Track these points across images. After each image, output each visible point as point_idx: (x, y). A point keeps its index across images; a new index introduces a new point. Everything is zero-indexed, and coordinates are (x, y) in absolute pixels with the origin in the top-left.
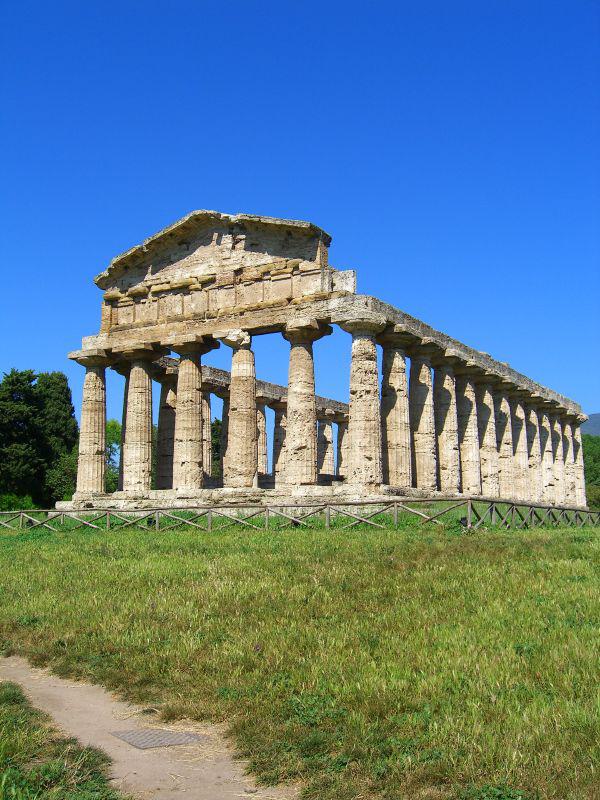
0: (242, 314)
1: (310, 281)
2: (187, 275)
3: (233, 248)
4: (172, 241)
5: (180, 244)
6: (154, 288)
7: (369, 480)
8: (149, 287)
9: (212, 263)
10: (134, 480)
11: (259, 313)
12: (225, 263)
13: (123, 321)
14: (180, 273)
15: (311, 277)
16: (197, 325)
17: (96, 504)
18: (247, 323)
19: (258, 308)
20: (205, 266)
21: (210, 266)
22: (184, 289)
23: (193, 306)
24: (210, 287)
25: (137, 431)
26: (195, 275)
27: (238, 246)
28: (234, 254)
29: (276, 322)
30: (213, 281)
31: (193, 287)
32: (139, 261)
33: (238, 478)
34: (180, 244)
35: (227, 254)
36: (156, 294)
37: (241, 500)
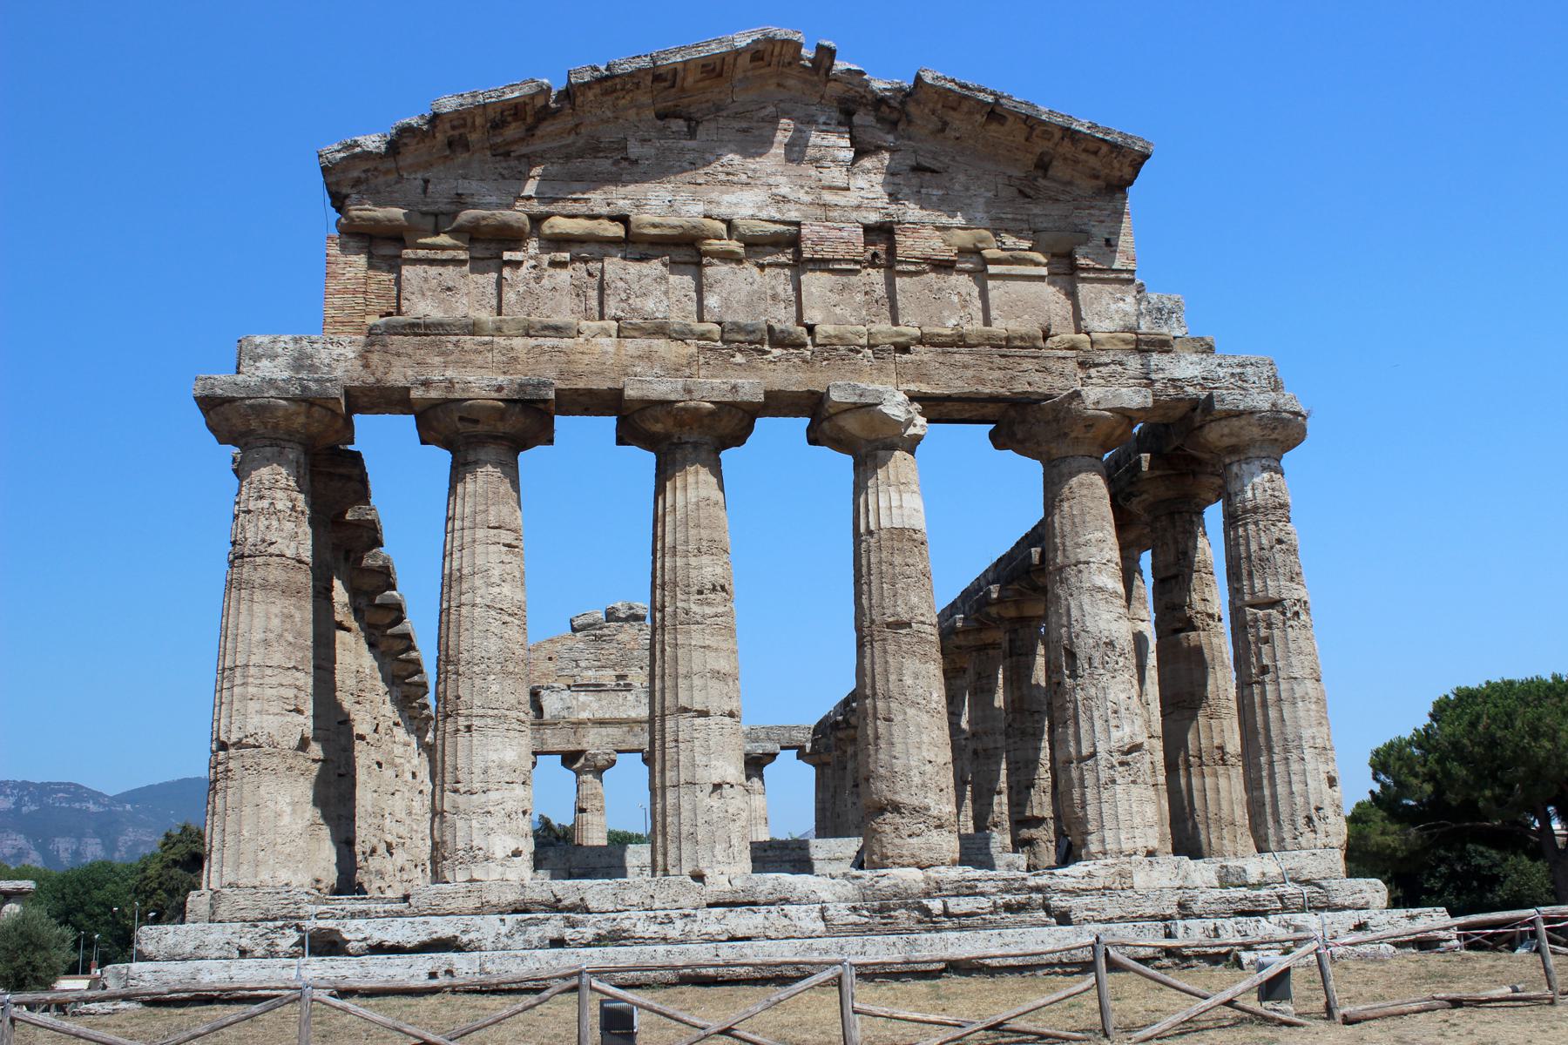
0: (904, 349)
1: (1106, 299)
4: (645, 99)
5: (662, 116)
9: (784, 190)
10: (501, 845)
11: (962, 356)
12: (828, 197)
13: (422, 307)
15: (1108, 288)
16: (739, 358)
17: (355, 931)
18: (922, 377)
19: (960, 341)
22: (685, 249)
24: (768, 259)
26: (724, 211)
27: (867, 163)
28: (860, 181)
29: (1020, 387)
31: (715, 245)
32: (513, 131)
33: (935, 837)
34: (662, 116)
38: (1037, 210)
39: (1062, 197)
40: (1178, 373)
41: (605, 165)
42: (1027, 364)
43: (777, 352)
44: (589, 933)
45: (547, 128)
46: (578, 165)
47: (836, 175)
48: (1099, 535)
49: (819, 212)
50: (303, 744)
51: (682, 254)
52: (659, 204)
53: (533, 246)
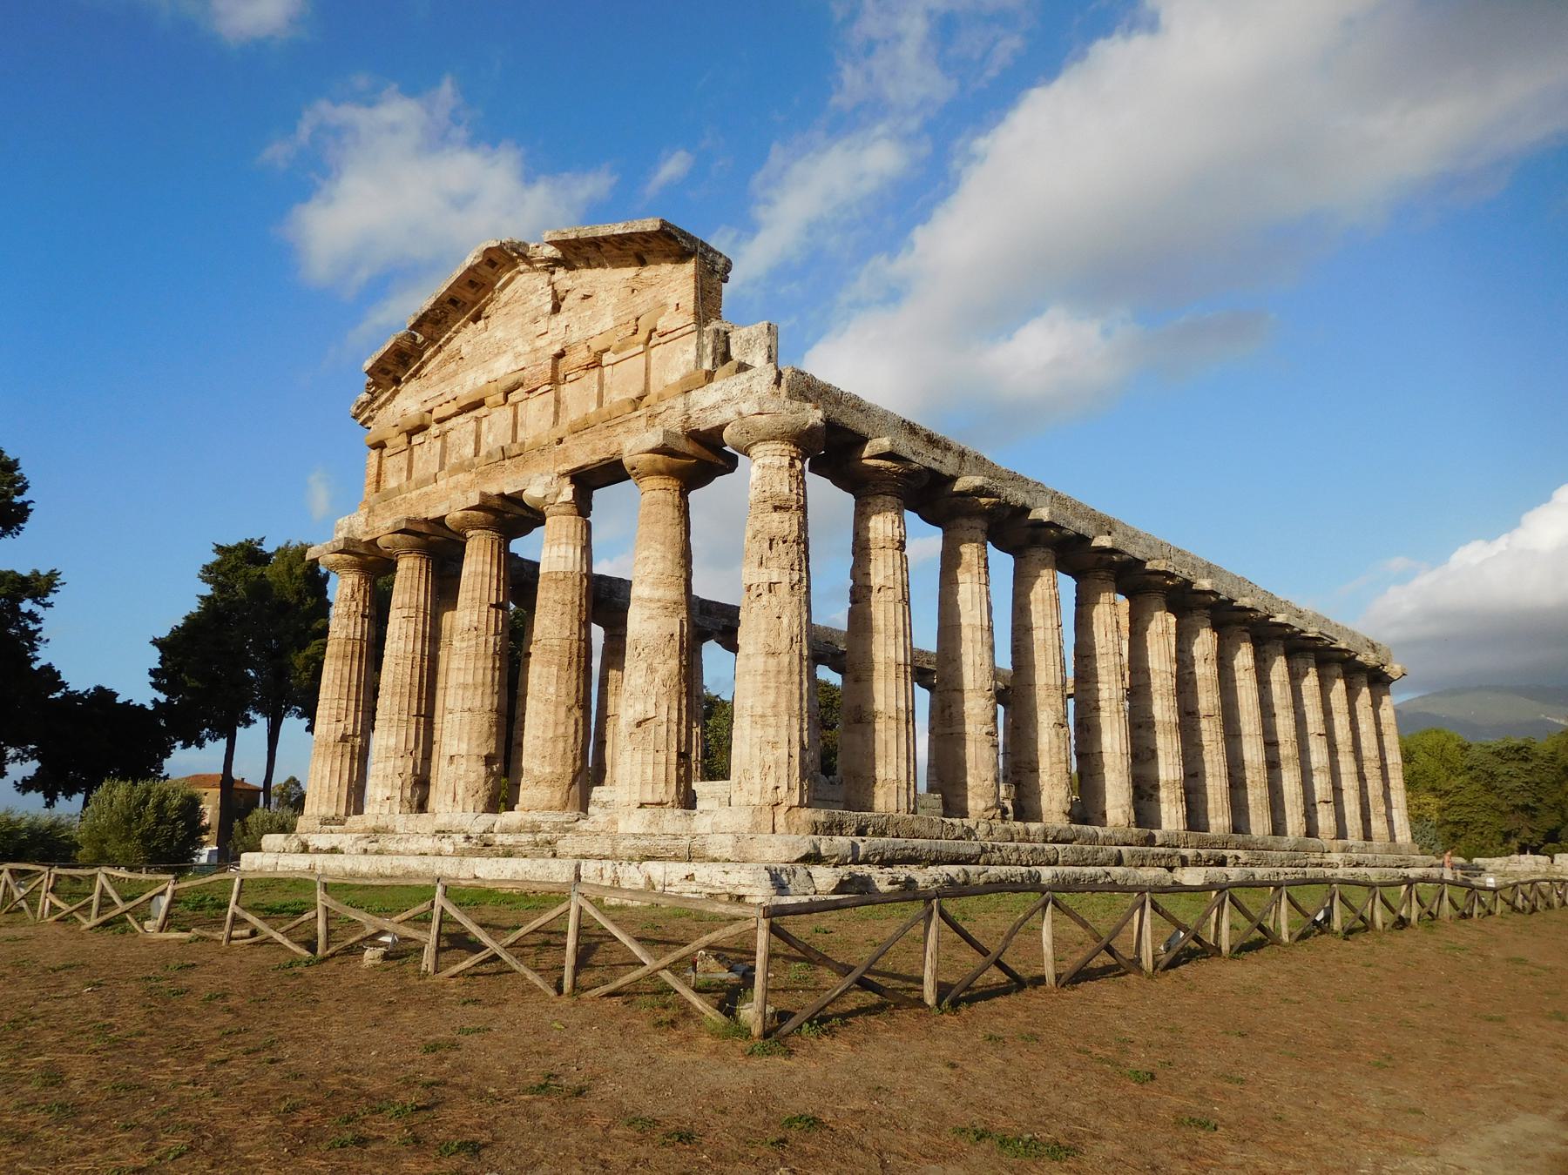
0: (560, 441)
2: (482, 381)
3: (556, 309)
6: (436, 415)
7: (769, 797)
8: (430, 412)
14: (473, 376)
18: (566, 459)
20: (508, 357)
21: (518, 356)
23: (490, 439)
25: (393, 694)
28: (553, 324)
30: (518, 385)
35: (542, 326)
36: (440, 421)
37: (526, 838)
38: (638, 300)
39: (654, 281)
40: (706, 405)
41: (452, 366)
42: (620, 429)
43: (507, 462)
44: (375, 846)
45: (427, 354)
46: (444, 371)
48: (646, 554)
49: (532, 356)
50: (344, 738)
51: (482, 411)
52: (469, 382)
53: (434, 429)
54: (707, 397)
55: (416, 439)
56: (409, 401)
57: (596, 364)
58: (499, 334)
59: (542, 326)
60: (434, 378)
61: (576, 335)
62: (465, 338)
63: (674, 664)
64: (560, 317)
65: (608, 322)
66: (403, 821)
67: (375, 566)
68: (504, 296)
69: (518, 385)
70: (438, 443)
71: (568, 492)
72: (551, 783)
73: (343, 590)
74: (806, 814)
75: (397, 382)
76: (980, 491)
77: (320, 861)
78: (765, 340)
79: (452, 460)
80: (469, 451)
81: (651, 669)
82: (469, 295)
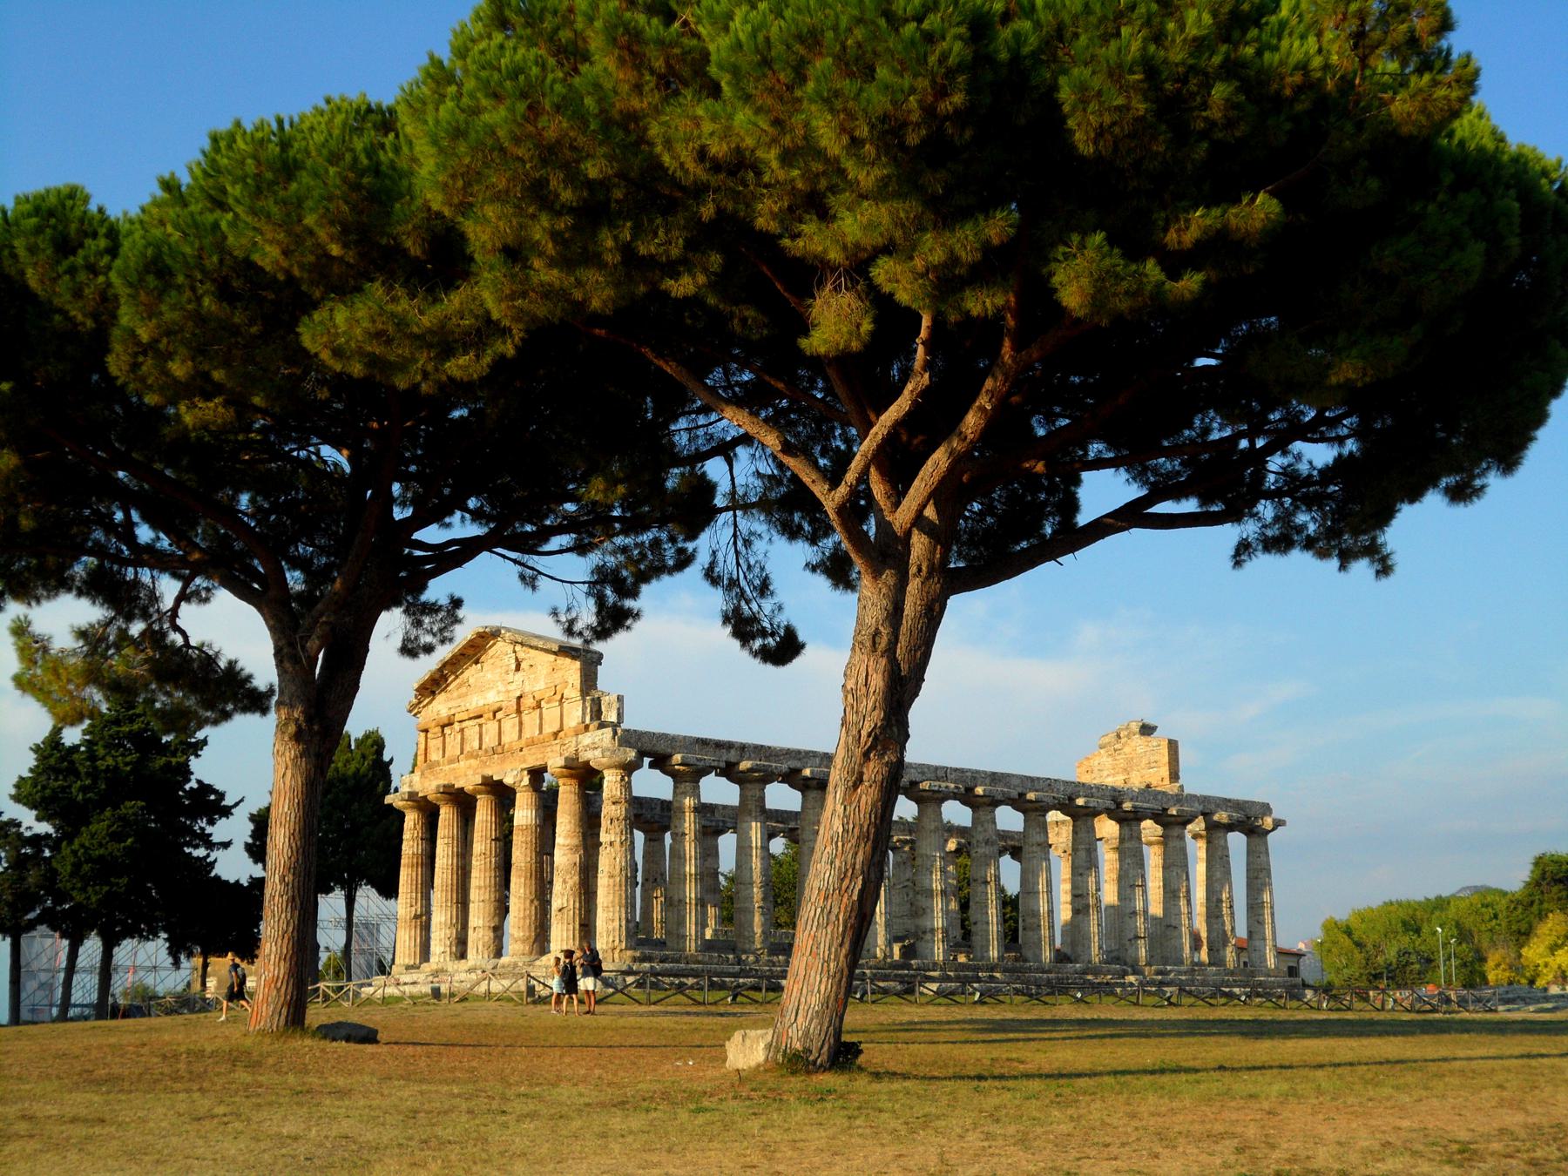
2: (481, 703)
3: (518, 668)
41: (464, 690)
47: (510, 677)
50: (416, 917)
52: (475, 702)
53: (457, 726)
54: (586, 739)
55: (447, 730)
56: (440, 706)
57: (539, 706)
58: (489, 676)
59: (510, 677)
60: (455, 694)
61: (527, 689)
62: (471, 673)
63: (576, 878)
64: (520, 674)
65: (541, 685)
66: (452, 966)
67: (430, 814)
68: (491, 652)
69: (500, 709)
70: (459, 736)
71: (526, 781)
72: (523, 942)
73: (411, 820)
74: (629, 953)
75: (433, 693)
76: (751, 770)
77: (407, 989)
78: (616, 705)
79: (467, 748)
80: (476, 745)
81: (565, 882)
82: (471, 652)
